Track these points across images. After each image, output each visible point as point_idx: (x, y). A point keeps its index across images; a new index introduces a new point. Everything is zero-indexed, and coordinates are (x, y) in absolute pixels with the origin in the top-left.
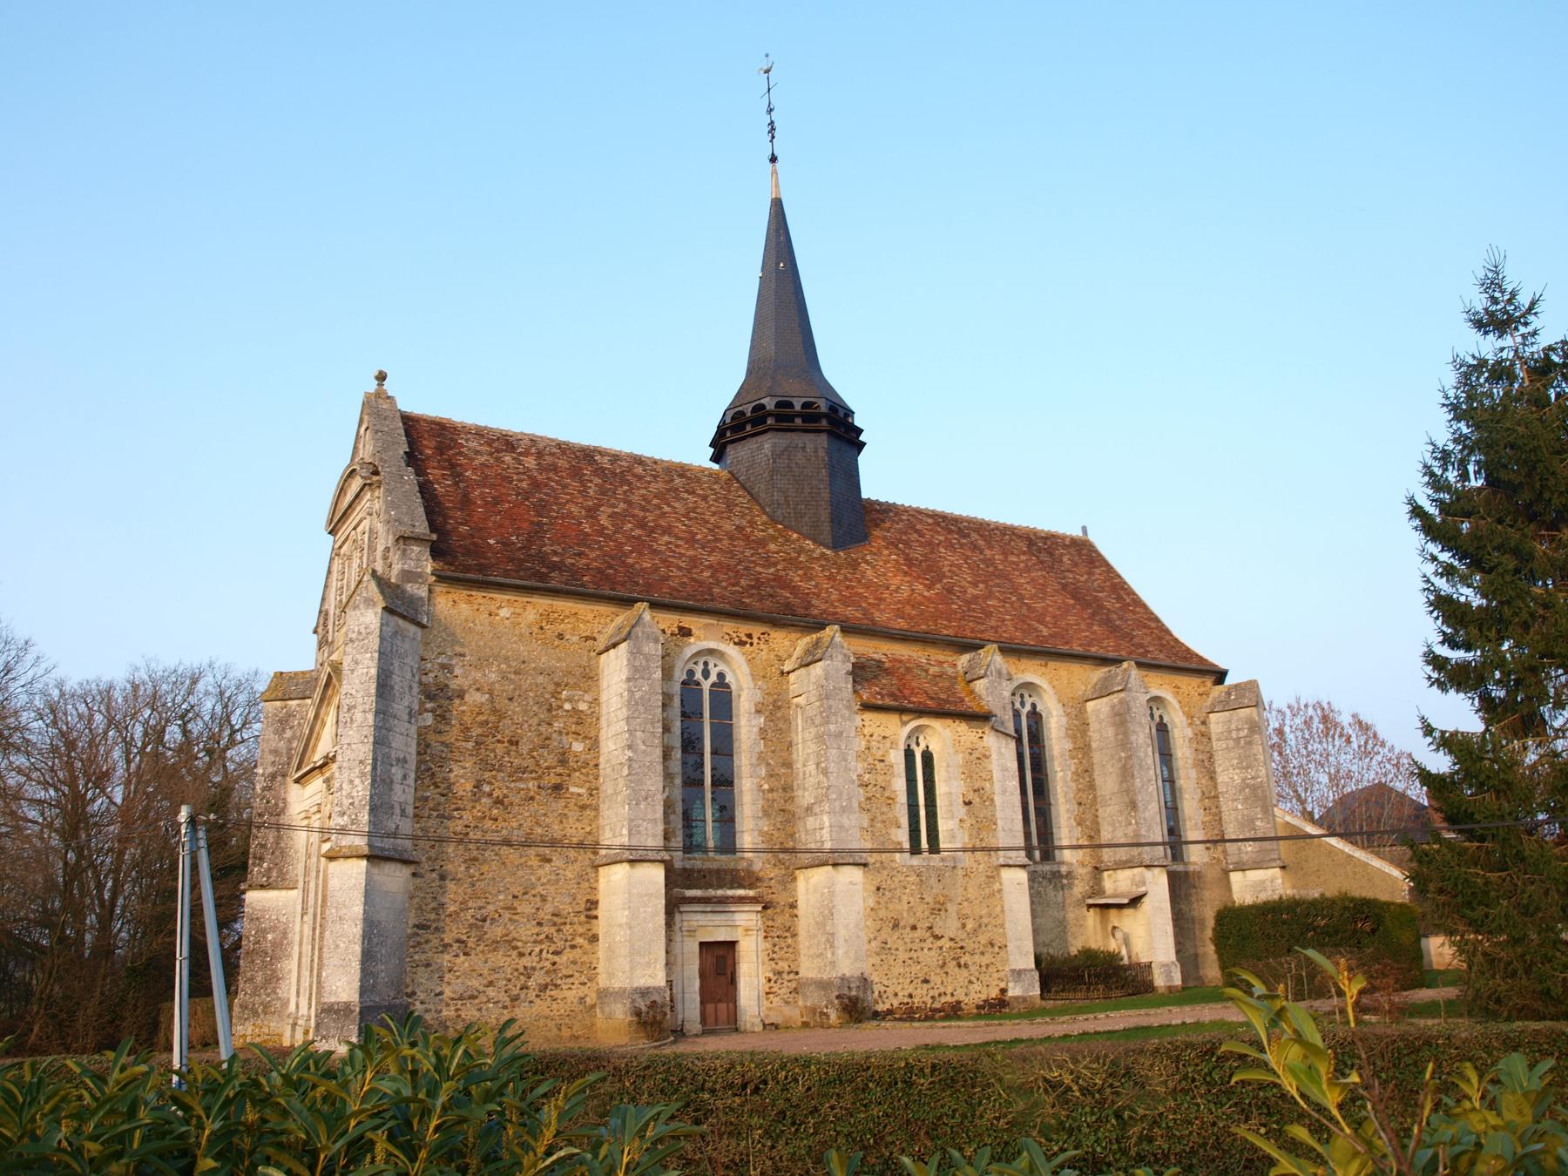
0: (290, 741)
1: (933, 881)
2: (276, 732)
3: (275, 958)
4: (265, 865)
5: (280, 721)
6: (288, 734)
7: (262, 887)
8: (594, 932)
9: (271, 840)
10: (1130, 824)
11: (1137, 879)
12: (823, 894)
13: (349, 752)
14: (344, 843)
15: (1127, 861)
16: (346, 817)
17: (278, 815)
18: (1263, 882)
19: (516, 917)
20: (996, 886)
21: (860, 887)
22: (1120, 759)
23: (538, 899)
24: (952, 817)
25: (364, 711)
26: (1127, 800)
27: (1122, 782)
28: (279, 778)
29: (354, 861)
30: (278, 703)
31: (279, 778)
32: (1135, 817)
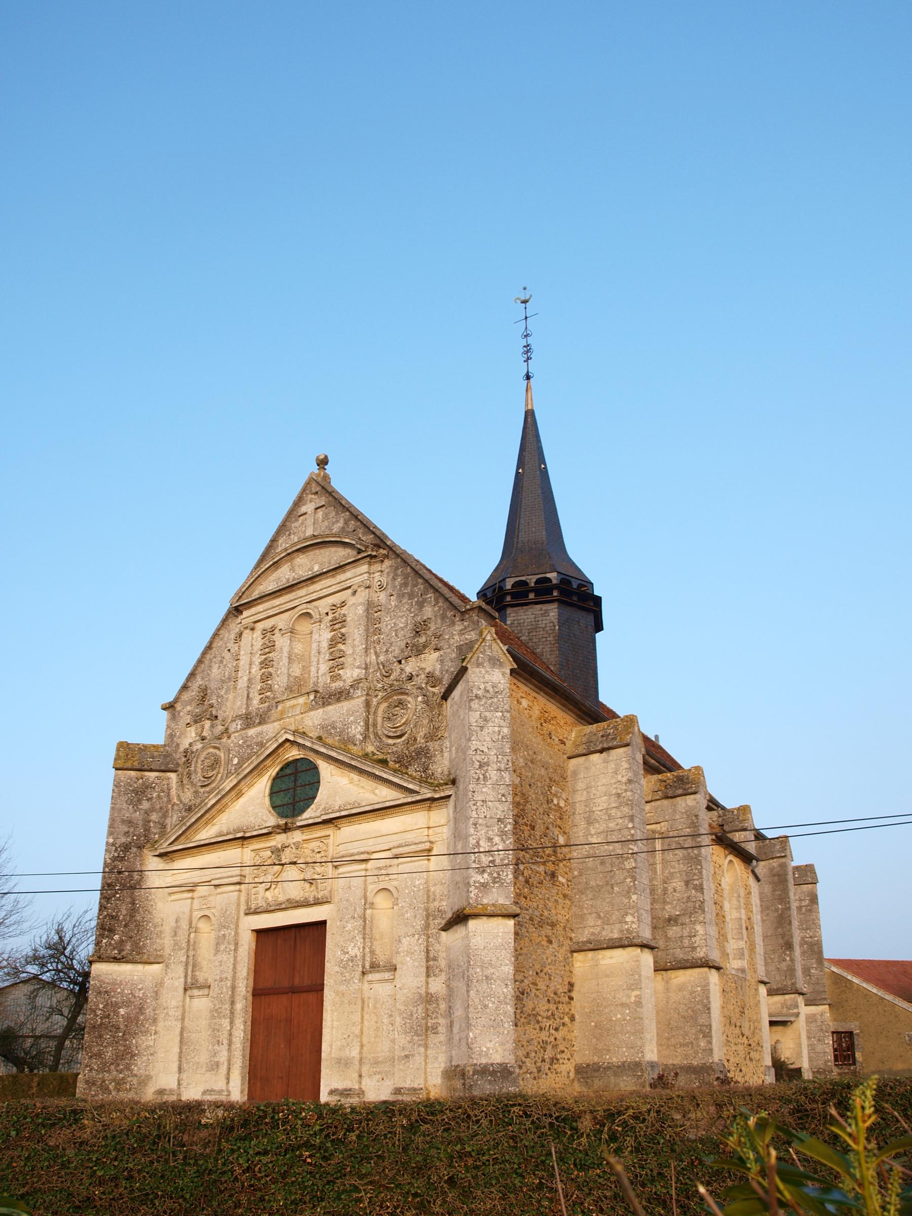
0: (147, 813)
1: (739, 989)
2: (130, 802)
3: (128, 1033)
4: (116, 937)
5: (136, 791)
6: (145, 805)
7: (116, 960)
8: (572, 1012)
9: (124, 912)
10: (785, 960)
11: (789, 1003)
12: (692, 993)
13: (484, 809)
14: (485, 901)
15: (778, 989)
16: (486, 875)
17: (133, 888)
18: (814, 1015)
19: (537, 992)
20: (758, 998)
21: (717, 987)
22: (777, 910)
23: (547, 977)
24: (743, 939)
25: (499, 770)
26: (781, 941)
27: (776, 928)
28: (134, 850)
29: (500, 920)
30: (133, 773)
31: (134, 850)
32: (790, 956)
